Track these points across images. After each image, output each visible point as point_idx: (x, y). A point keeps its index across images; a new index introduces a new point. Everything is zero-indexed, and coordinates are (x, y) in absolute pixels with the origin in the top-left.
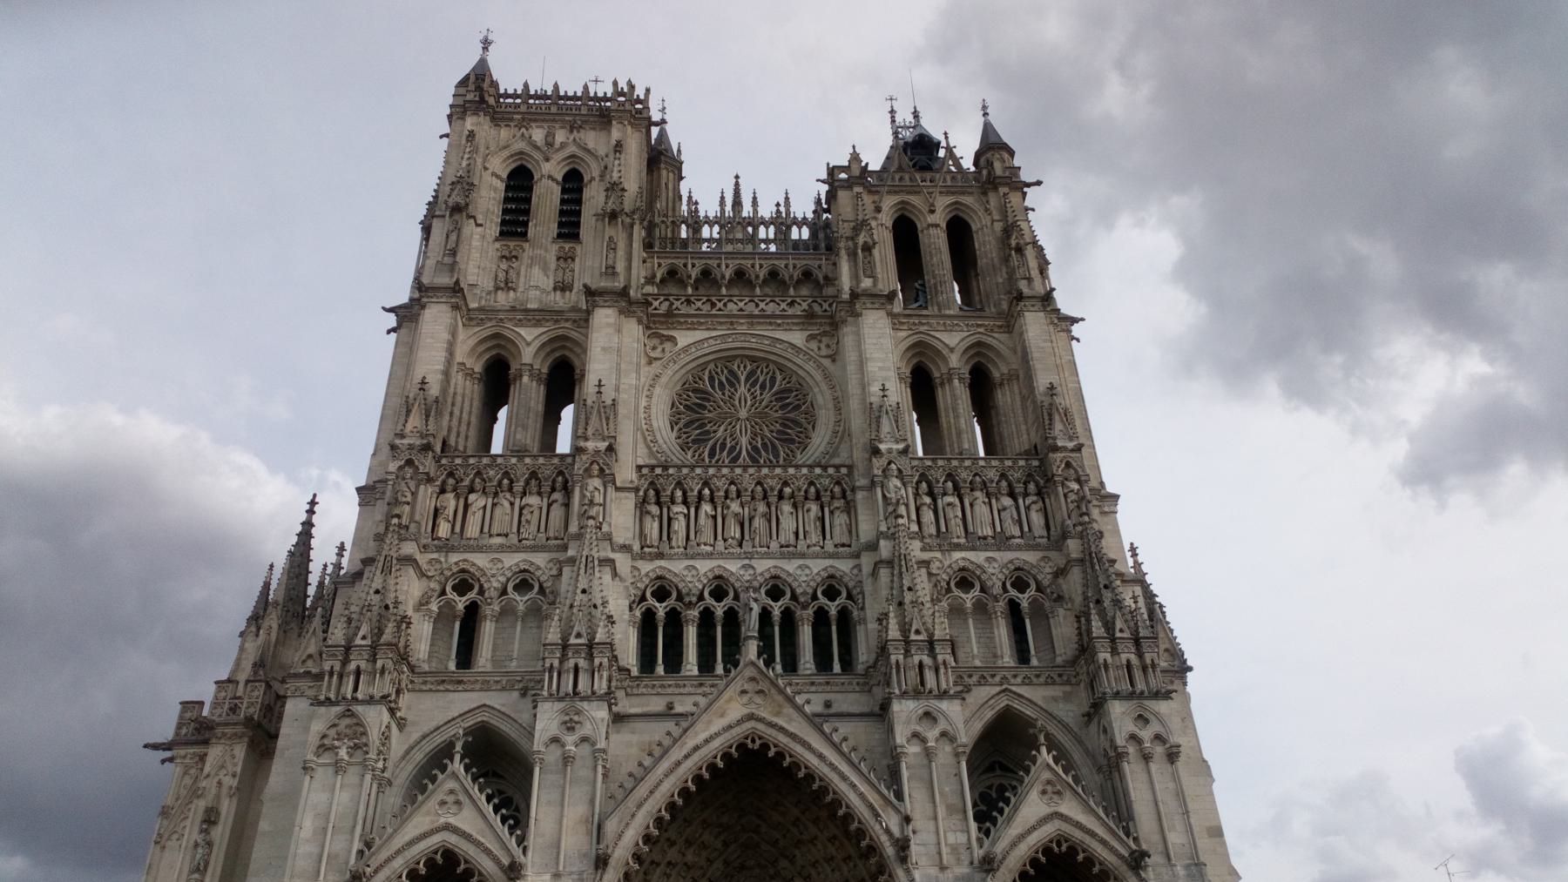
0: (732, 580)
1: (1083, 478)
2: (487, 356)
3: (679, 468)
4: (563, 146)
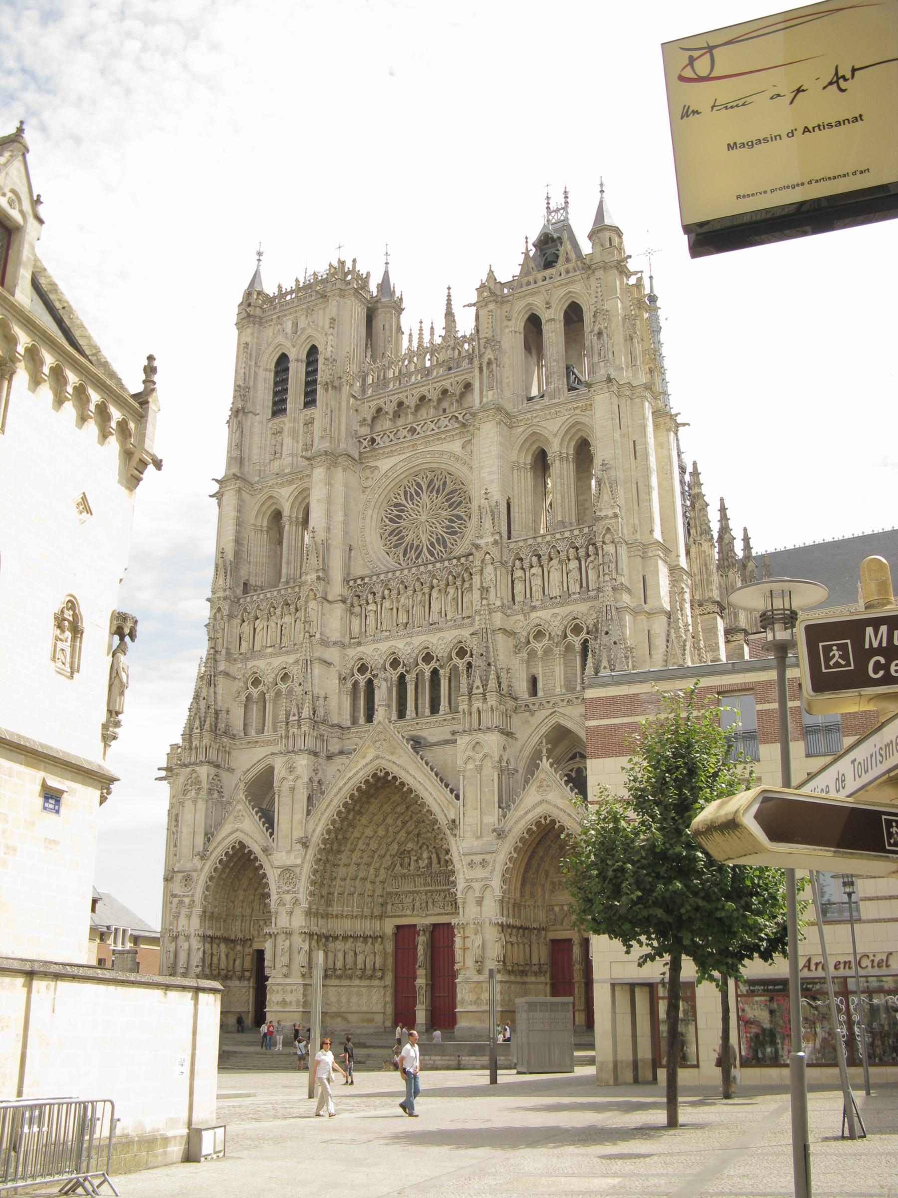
0: (400, 654)
1: (616, 540)
2: (269, 512)
3: (371, 577)
4: (304, 329)
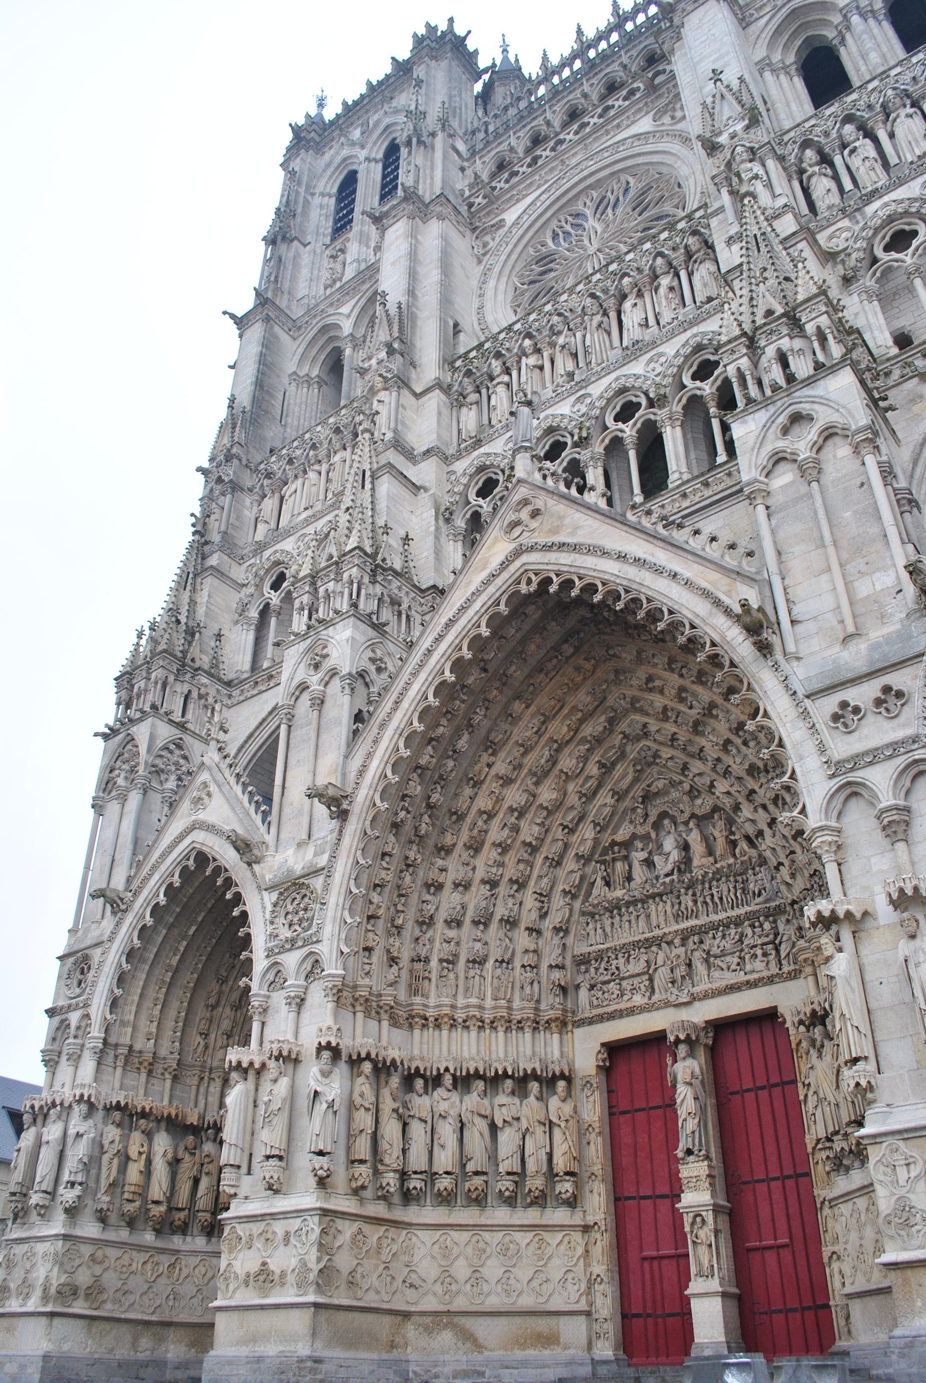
2: (323, 357)
